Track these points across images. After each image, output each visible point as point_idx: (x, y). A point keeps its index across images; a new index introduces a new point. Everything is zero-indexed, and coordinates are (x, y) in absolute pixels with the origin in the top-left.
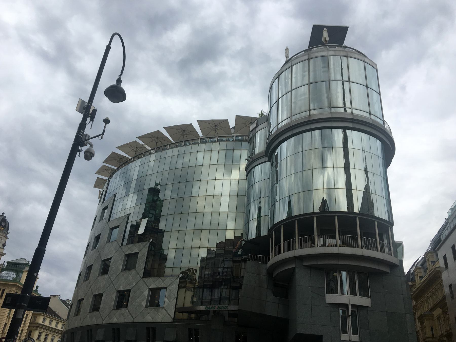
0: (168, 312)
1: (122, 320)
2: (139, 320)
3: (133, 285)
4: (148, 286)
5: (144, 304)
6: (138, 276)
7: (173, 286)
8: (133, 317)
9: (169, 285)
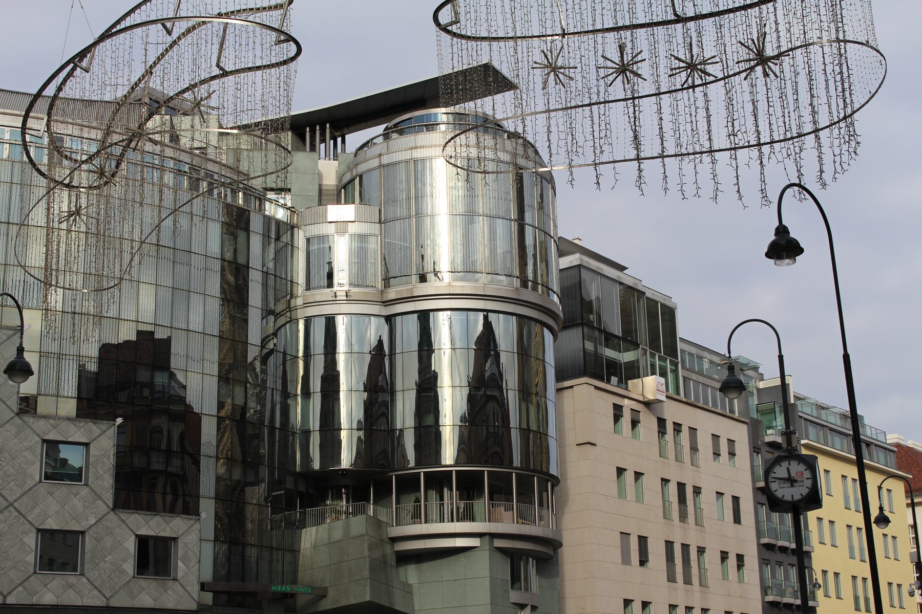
0: (188, 589)
1: (72, 599)
3: (88, 522)
4: (131, 530)
5: (130, 567)
6: (99, 502)
7: (190, 537)
8: (104, 596)
9: (182, 534)
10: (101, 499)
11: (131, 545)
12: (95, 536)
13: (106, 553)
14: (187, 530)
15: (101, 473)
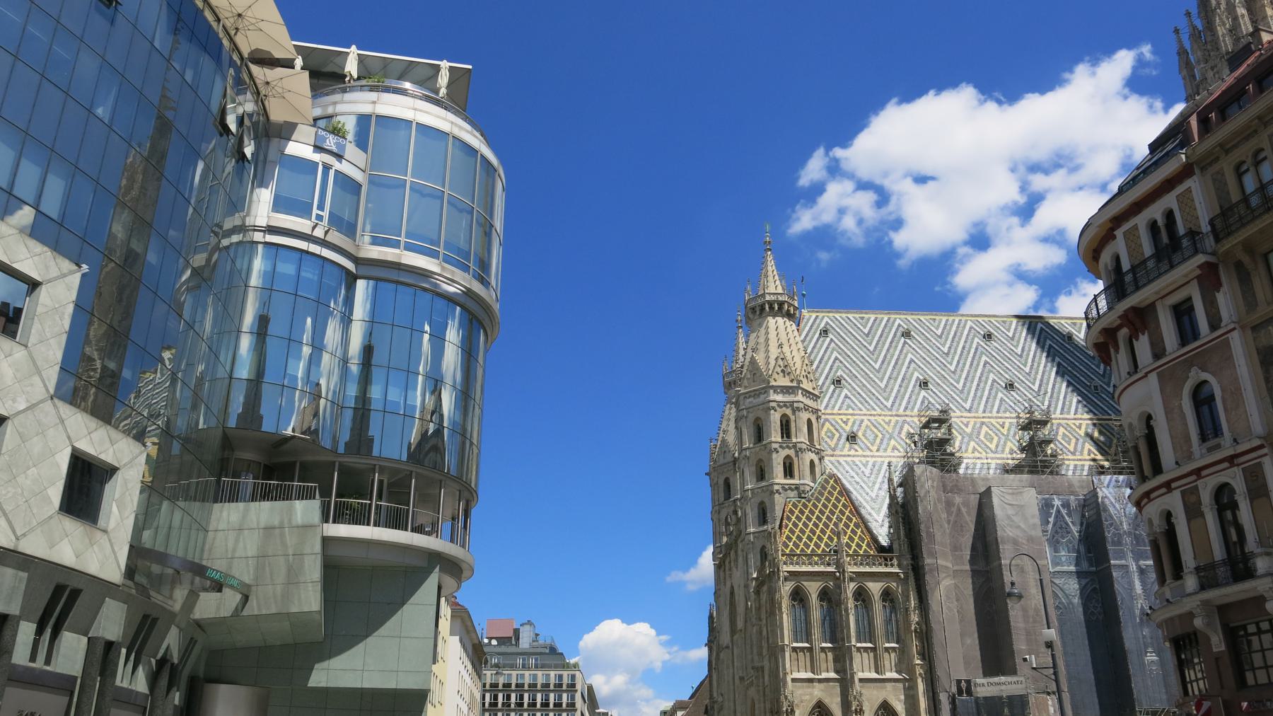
0: (116, 549)
2: (34, 546)
3: (16, 405)
4: (69, 438)
5: (56, 494)
6: (36, 379)
9: (125, 465)
10: (39, 373)
11: (63, 462)
12: (21, 430)
13: (31, 463)
14: (130, 462)
15: (48, 335)
